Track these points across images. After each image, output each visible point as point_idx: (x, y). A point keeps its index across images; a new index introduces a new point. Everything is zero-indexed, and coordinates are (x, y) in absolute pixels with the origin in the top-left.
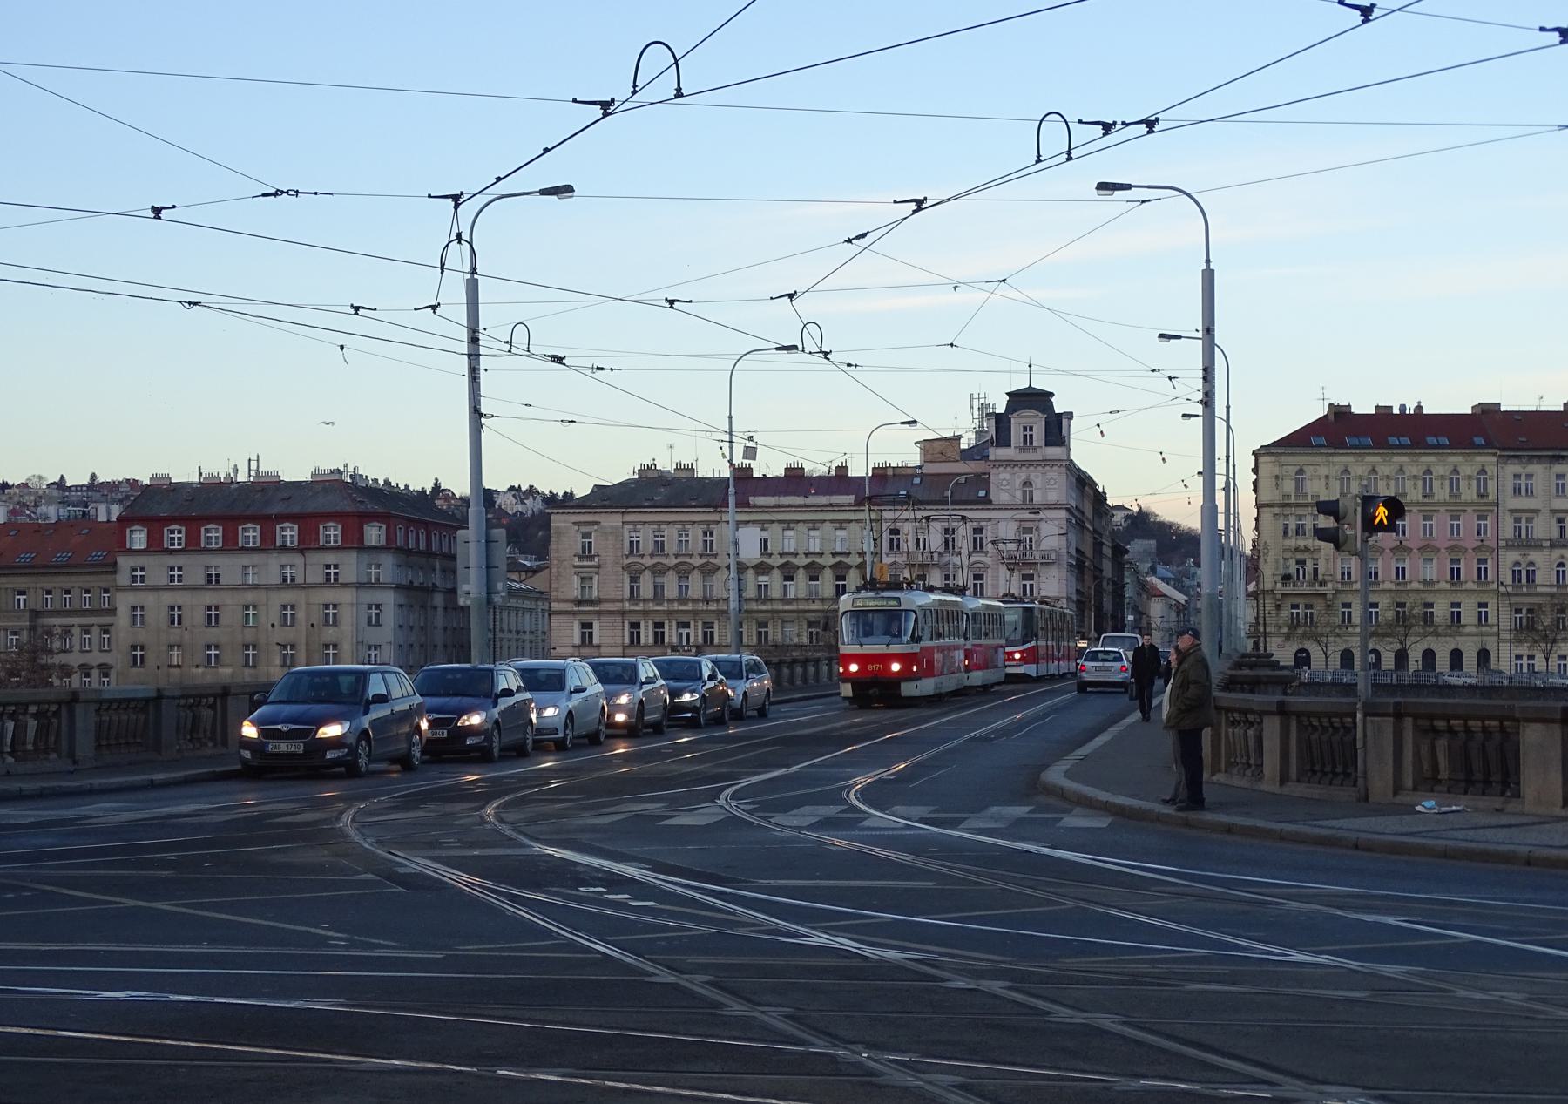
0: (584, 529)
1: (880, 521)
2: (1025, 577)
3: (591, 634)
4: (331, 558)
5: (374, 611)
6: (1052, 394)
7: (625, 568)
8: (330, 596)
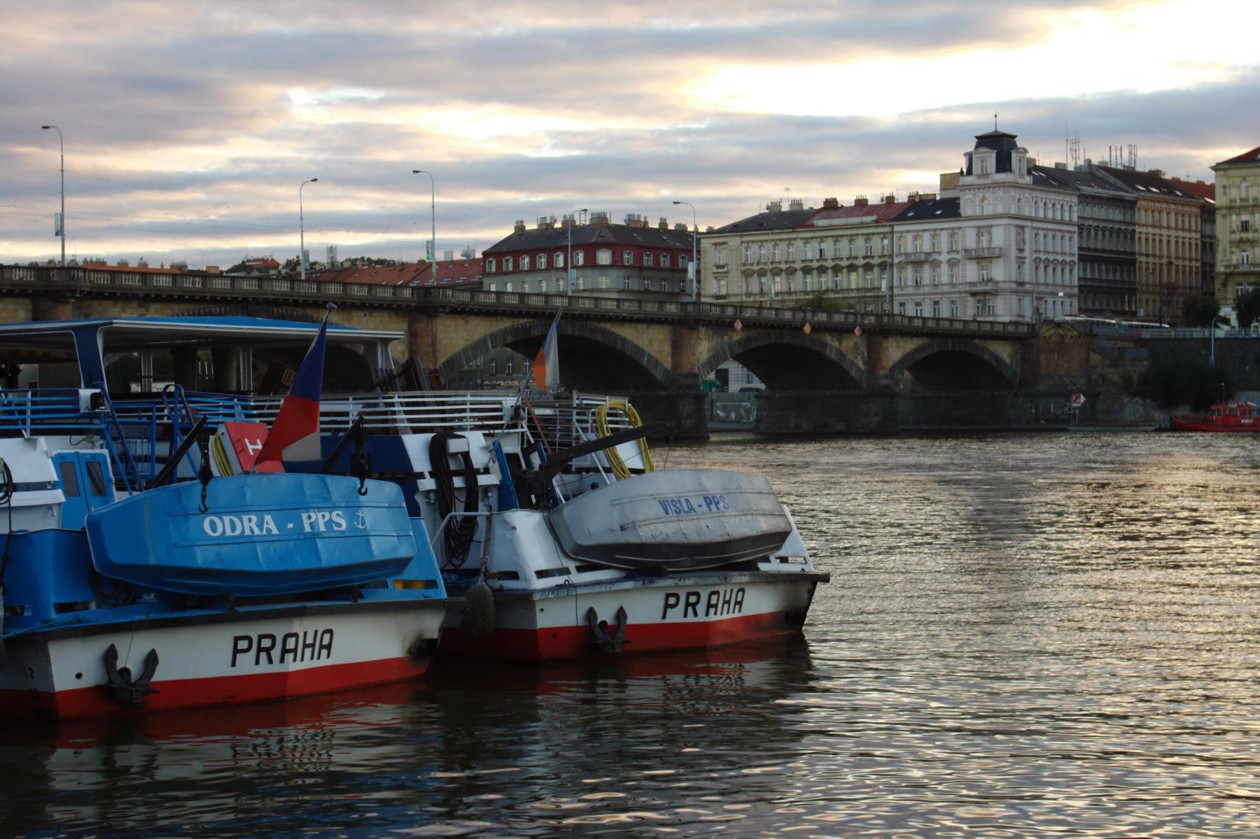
1: (892, 233)
6: (1014, 137)
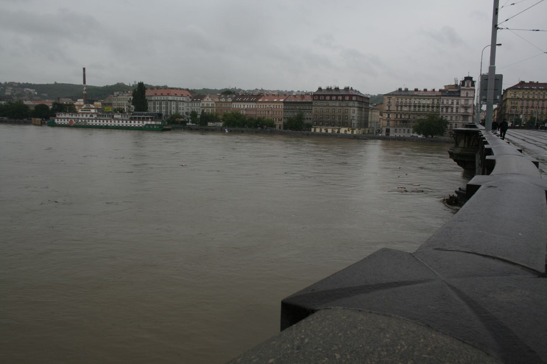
0: (389, 98)
1: (440, 99)
2: (465, 109)
3: (389, 116)
4: (347, 102)
5: (353, 111)
6: (472, 77)
7: (396, 105)
8: (347, 108)
